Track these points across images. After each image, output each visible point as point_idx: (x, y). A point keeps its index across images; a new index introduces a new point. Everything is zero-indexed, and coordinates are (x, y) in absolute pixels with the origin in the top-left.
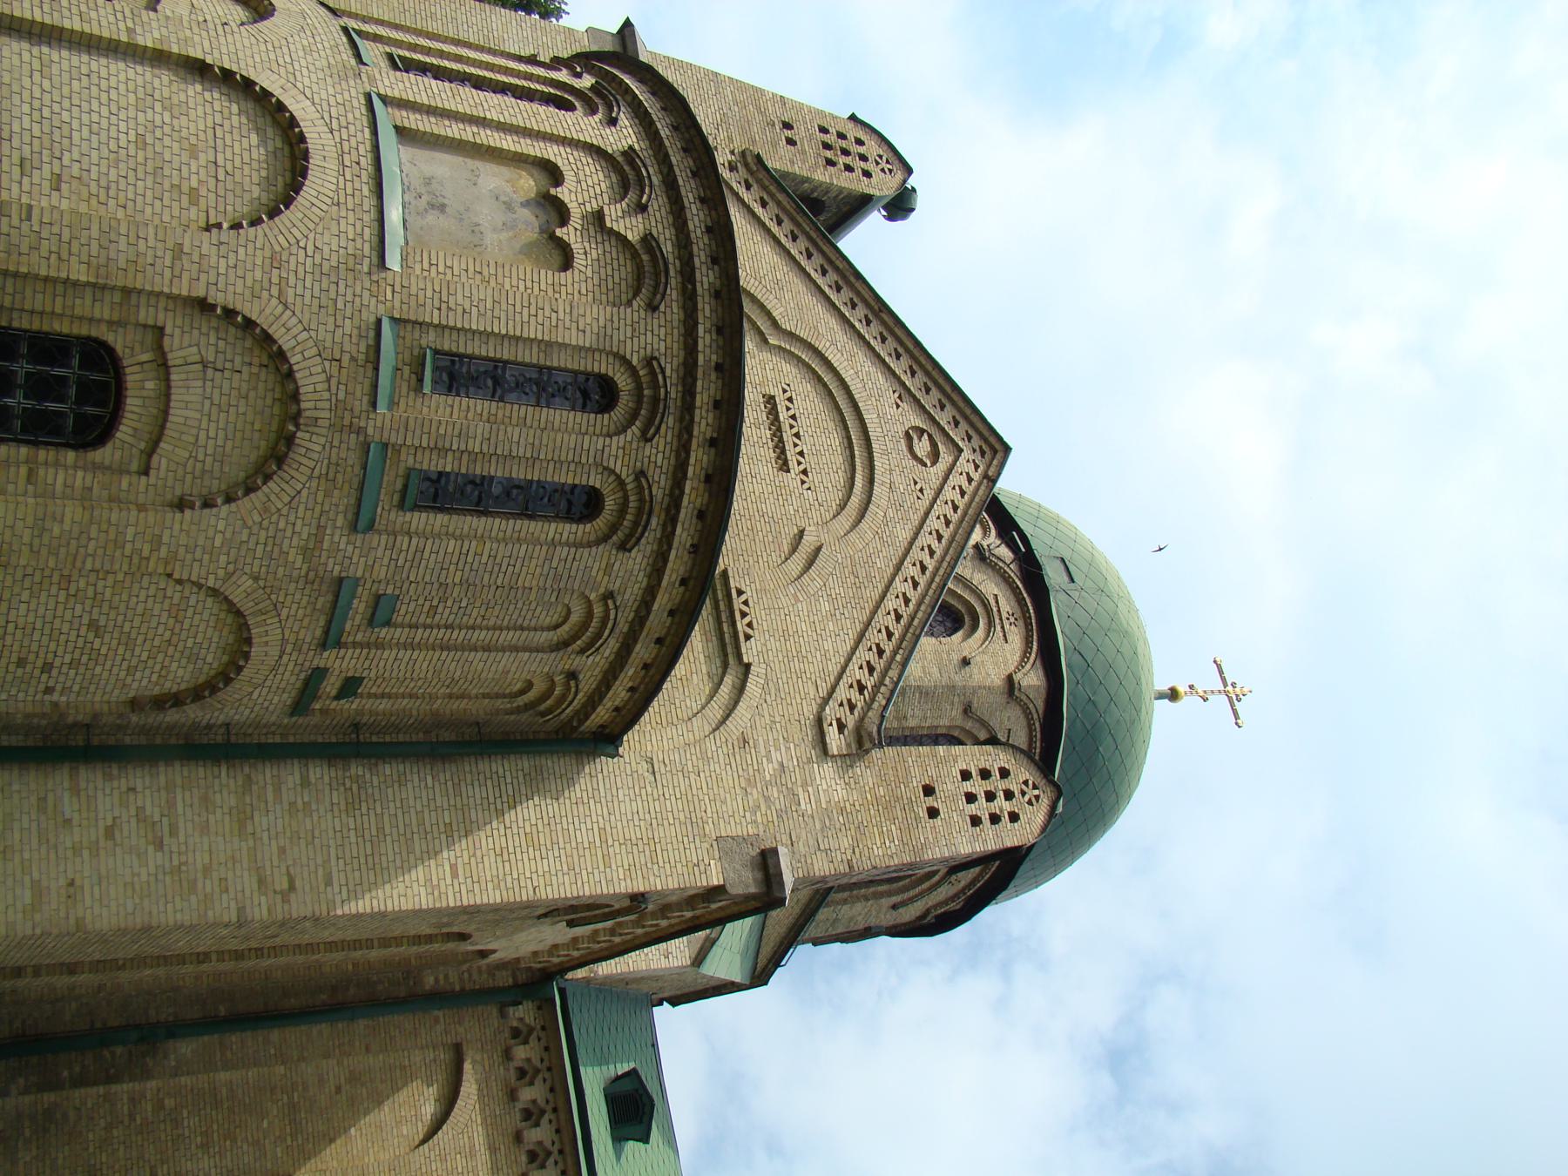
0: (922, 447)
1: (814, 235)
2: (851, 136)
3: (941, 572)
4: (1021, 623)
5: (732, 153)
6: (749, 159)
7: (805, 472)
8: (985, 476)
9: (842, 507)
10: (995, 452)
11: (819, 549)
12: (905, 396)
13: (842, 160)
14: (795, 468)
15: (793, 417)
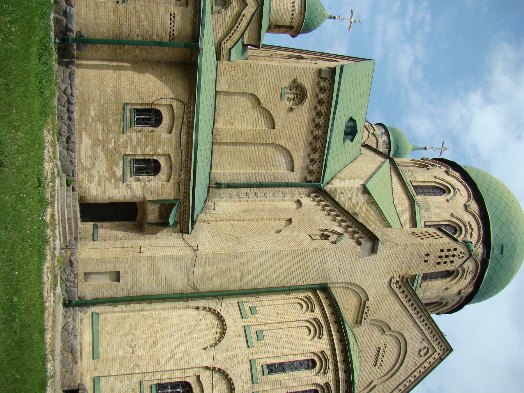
0: (422, 353)
1: (416, 300)
2: (449, 264)
3: (410, 388)
4: (473, 274)
5: (400, 276)
6: (404, 280)
7: (381, 366)
8: (440, 357)
9: (389, 372)
10: (448, 349)
11: (375, 386)
12: (425, 339)
13: (447, 253)
14: (378, 364)
15: (384, 352)
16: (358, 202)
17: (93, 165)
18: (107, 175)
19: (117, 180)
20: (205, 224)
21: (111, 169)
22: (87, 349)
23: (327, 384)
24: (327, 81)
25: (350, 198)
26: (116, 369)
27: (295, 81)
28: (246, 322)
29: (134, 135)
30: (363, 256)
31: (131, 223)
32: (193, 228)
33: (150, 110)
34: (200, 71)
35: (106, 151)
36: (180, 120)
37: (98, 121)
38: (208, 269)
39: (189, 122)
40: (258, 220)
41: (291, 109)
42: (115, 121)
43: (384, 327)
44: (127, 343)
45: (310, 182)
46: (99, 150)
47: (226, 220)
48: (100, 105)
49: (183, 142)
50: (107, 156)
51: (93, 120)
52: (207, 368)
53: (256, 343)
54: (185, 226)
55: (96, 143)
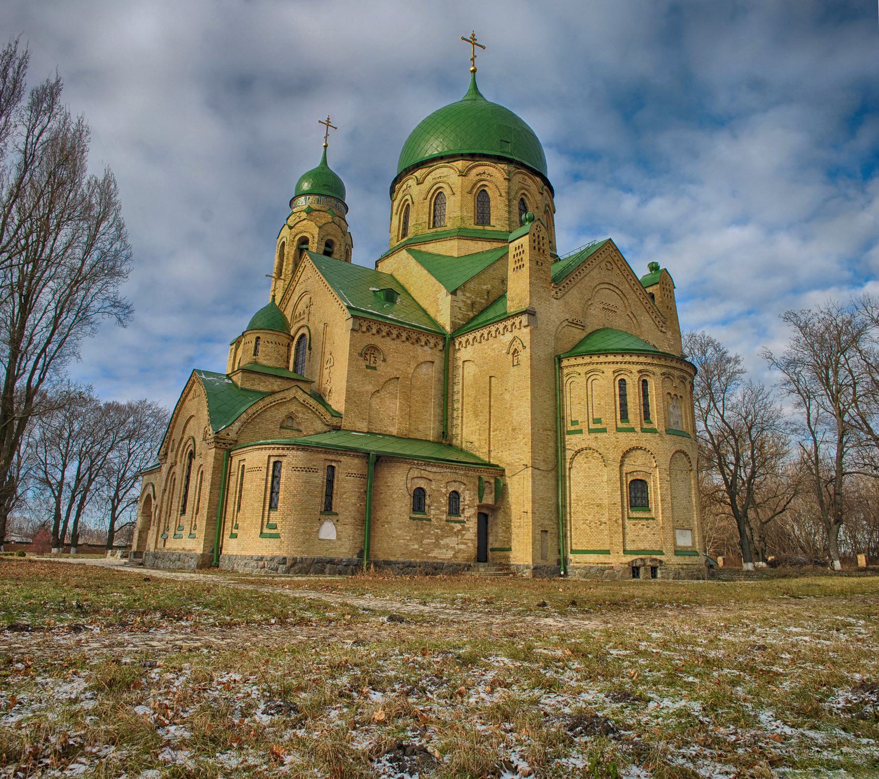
19: (464, 528)
22: (602, 558)
23: (640, 372)
26: (618, 538)
27: (361, 355)
28: (585, 430)
29: (433, 512)
30: (536, 322)
31: (490, 519)
36: (423, 472)
38: (541, 458)
40: (490, 406)
41: (384, 360)
42: (422, 528)
43: (587, 304)
44: (596, 527)
45: (444, 346)
46: (442, 542)
47: (489, 435)
48: (411, 540)
51: (420, 547)
52: (621, 466)
53: (604, 426)
54: (499, 472)
55: (437, 545)
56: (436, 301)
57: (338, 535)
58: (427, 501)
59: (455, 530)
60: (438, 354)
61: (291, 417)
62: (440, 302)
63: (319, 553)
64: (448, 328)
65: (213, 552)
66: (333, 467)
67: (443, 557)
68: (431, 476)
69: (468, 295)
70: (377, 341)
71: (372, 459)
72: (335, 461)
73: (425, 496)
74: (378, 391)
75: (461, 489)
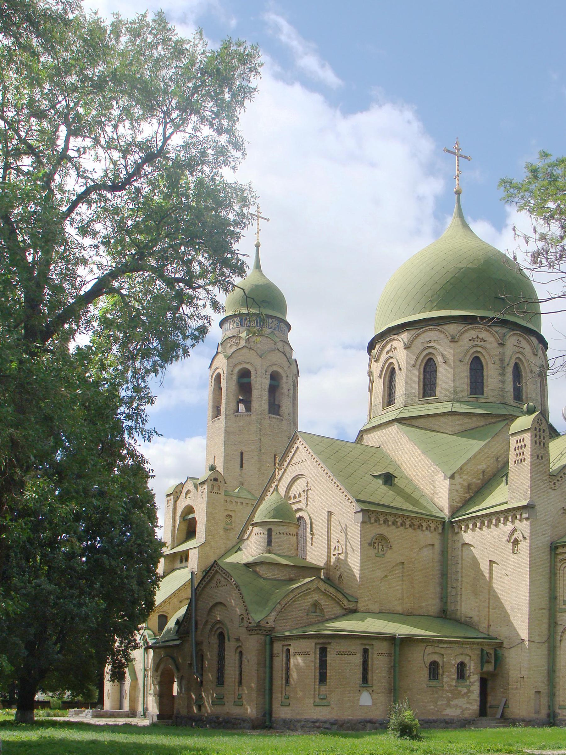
16: (460, 484)
17: (461, 707)
18: (466, 698)
19: (469, 691)
20: (491, 628)
21: (463, 695)
24: (371, 516)
25: (457, 491)
29: (445, 680)
32: (496, 638)
33: (430, 669)
34: (409, 635)
35: (453, 698)
36: (436, 648)
37: (436, 703)
39: (438, 642)
42: (437, 693)
46: (452, 703)
47: (489, 612)
49: (448, 646)
50: (456, 698)
55: (448, 705)
56: (433, 483)
57: (373, 702)
58: (441, 672)
59: (463, 693)
60: (438, 537)
61: (316, 605)
62: (437, 484)
63: (360, 715)
64: (447, 511)
65: (264, 715)
66: (368, 649)
67: (453, 714)
68: (443, 651)
69: (465, 477)
70: (383, 530)
71: (398, 642)
72: (369, 645)
73: (438, 667)
74: (386, 576)
75: (467, 660)
